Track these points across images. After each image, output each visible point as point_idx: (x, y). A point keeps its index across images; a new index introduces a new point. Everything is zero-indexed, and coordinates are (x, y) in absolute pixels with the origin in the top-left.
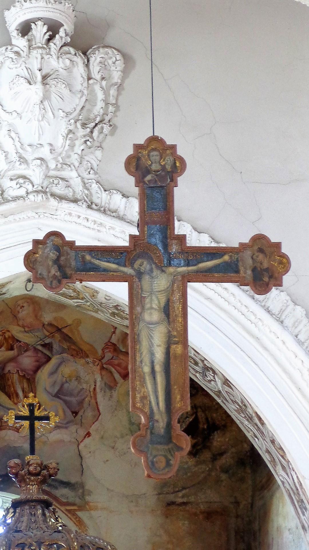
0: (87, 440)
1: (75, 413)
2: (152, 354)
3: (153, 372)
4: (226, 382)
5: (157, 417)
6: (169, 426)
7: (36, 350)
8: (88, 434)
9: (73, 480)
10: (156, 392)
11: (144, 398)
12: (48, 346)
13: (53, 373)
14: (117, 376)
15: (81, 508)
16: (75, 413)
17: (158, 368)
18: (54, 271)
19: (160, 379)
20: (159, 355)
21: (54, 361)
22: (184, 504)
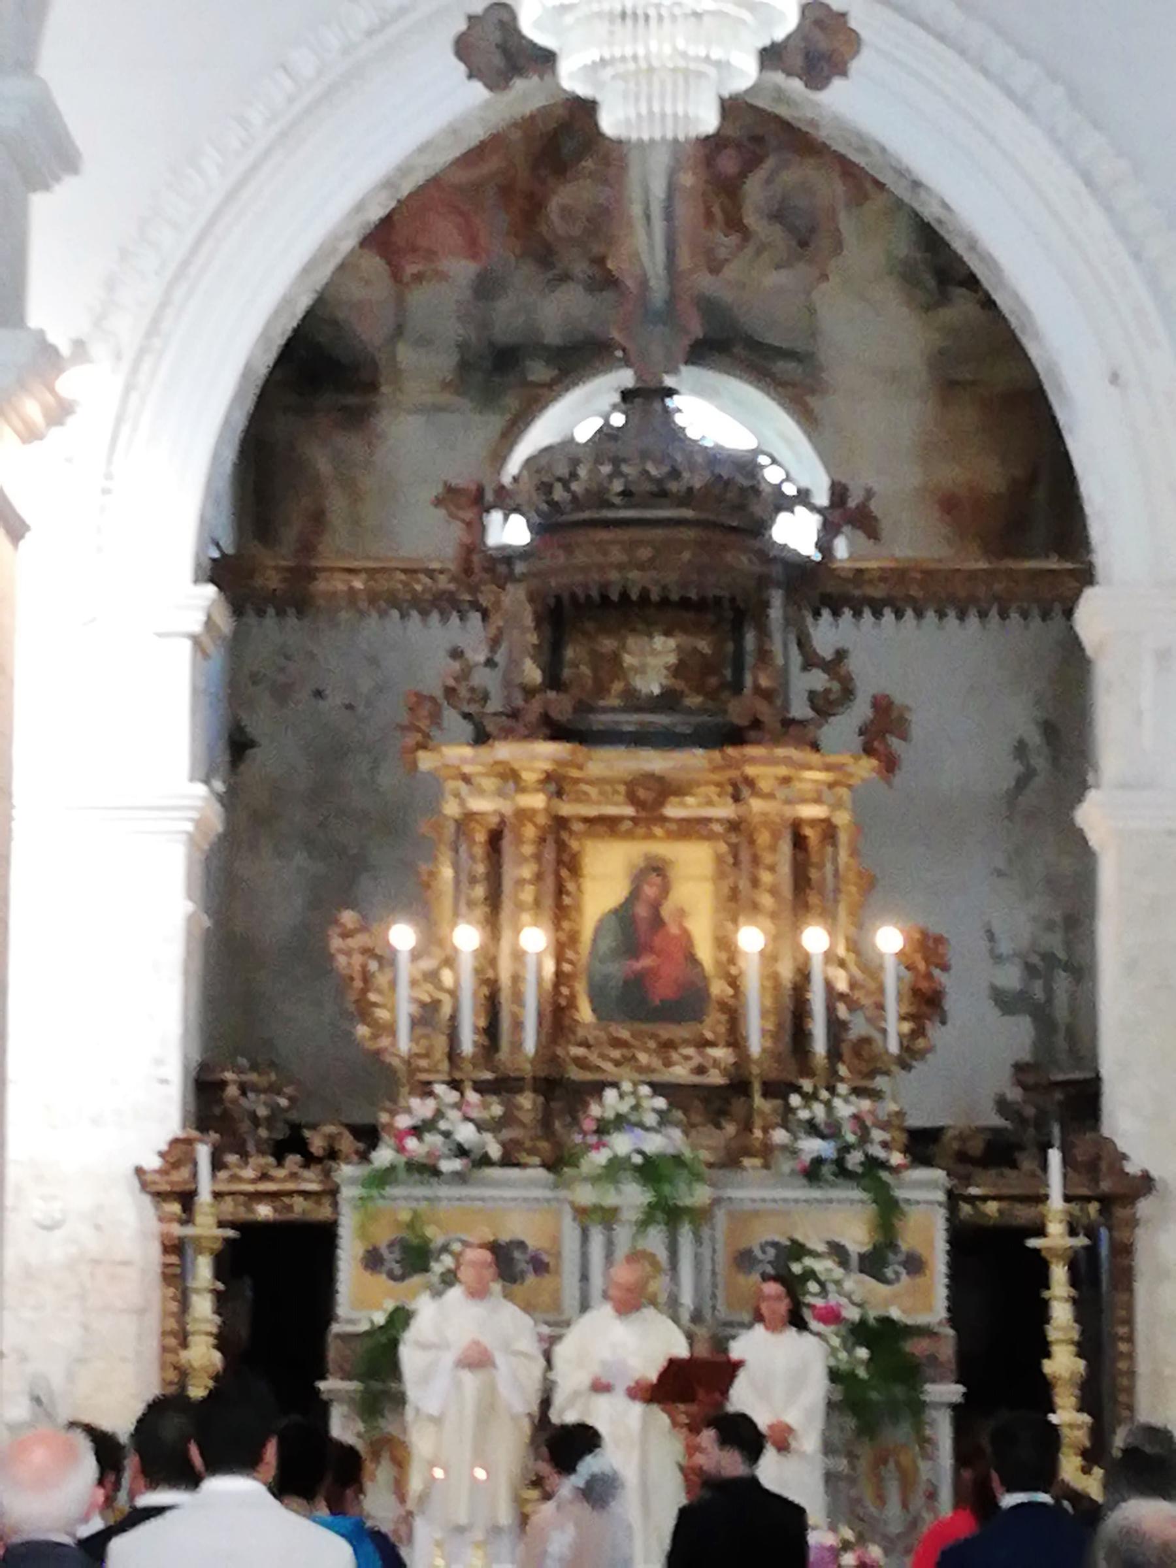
0: (824, 286)
1: (803, 244)
2: (646, 190)
3: (648, 217)
4: (945, 206)
5: (653, 283)
6: (672, 299)
7: (739, 146)
8: (824, 277)
9: (800, 346)
10: (651, 247)
11: (636, 255)
12: (758, 140)
13: (769, 181)
14: (869, 186)
15: (813, 392)
16: (803, 244)
17: (657, 211)
18: (498, 60)
19: (659, 225)
20: (658, 189)
21: (770, 163)
22: (973, 383)
